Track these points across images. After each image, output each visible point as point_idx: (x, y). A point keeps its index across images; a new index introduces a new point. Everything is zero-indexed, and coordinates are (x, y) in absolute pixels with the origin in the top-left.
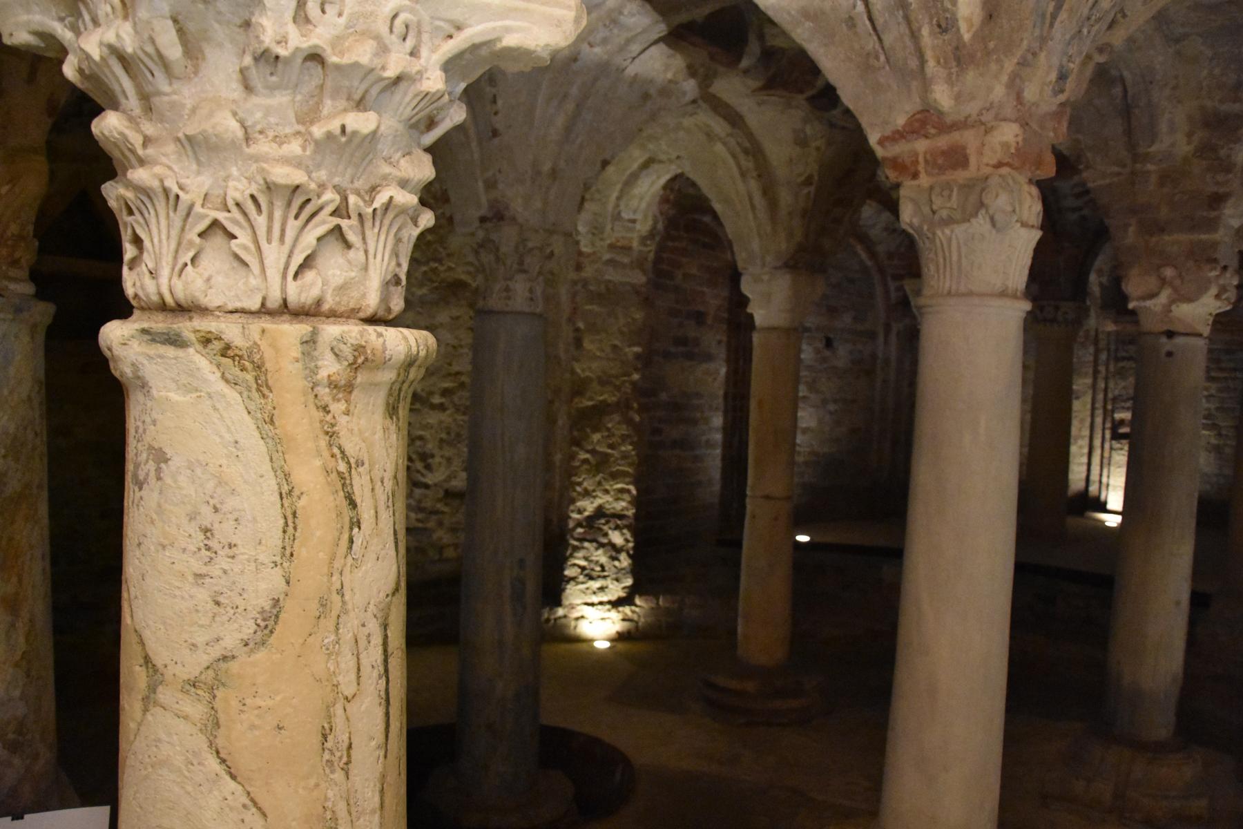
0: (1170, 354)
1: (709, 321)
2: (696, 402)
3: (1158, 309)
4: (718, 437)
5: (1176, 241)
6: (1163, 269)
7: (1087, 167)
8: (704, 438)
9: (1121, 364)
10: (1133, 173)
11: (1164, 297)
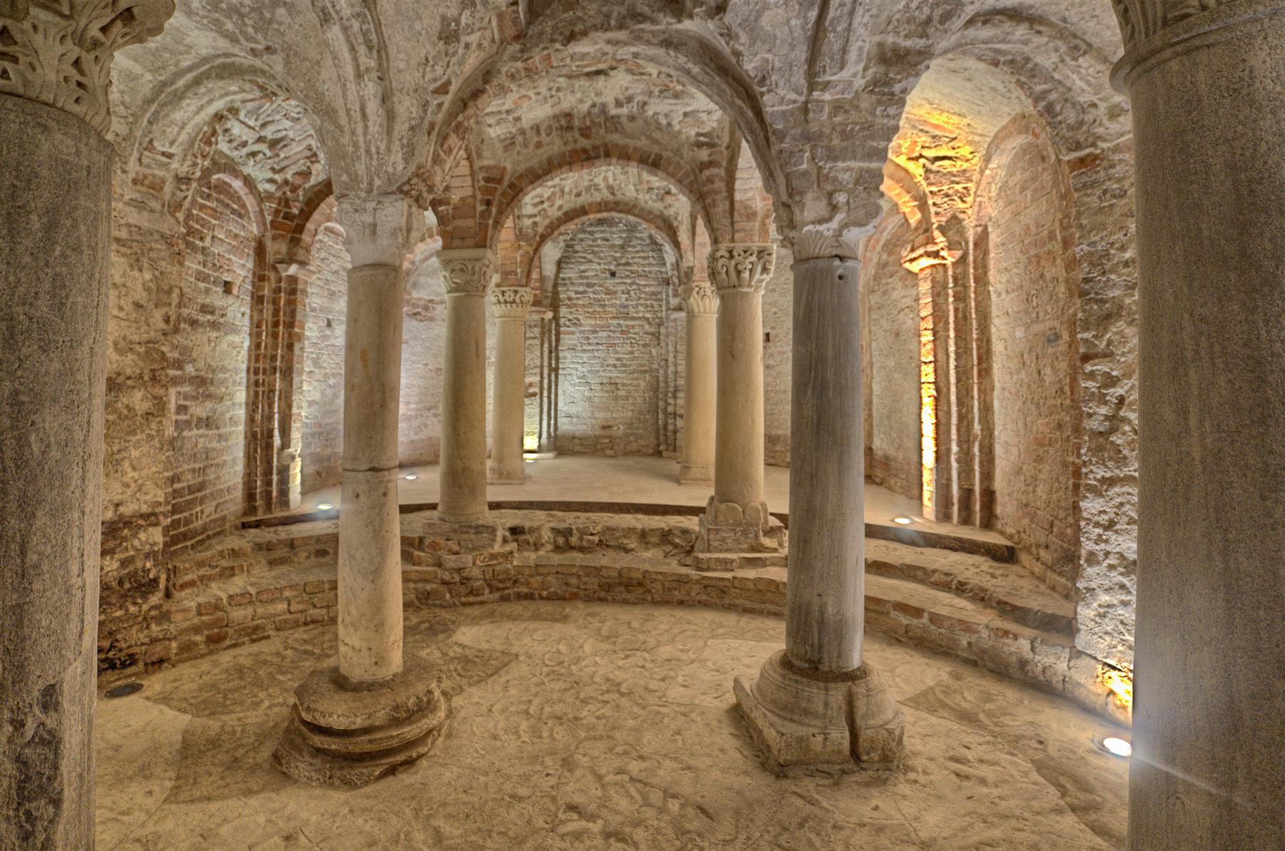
0: (840, 277)
1: (235, 291)
2: (221, 376)
3: (831, 233)
4: (241, 413)
5: (846, 170)
6: (836, 195)
7: (769, 91)
8: (228, 415)
9: (529, 342)
10: (806, 102)
11: (835, 224)
